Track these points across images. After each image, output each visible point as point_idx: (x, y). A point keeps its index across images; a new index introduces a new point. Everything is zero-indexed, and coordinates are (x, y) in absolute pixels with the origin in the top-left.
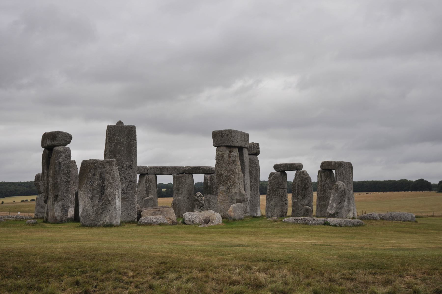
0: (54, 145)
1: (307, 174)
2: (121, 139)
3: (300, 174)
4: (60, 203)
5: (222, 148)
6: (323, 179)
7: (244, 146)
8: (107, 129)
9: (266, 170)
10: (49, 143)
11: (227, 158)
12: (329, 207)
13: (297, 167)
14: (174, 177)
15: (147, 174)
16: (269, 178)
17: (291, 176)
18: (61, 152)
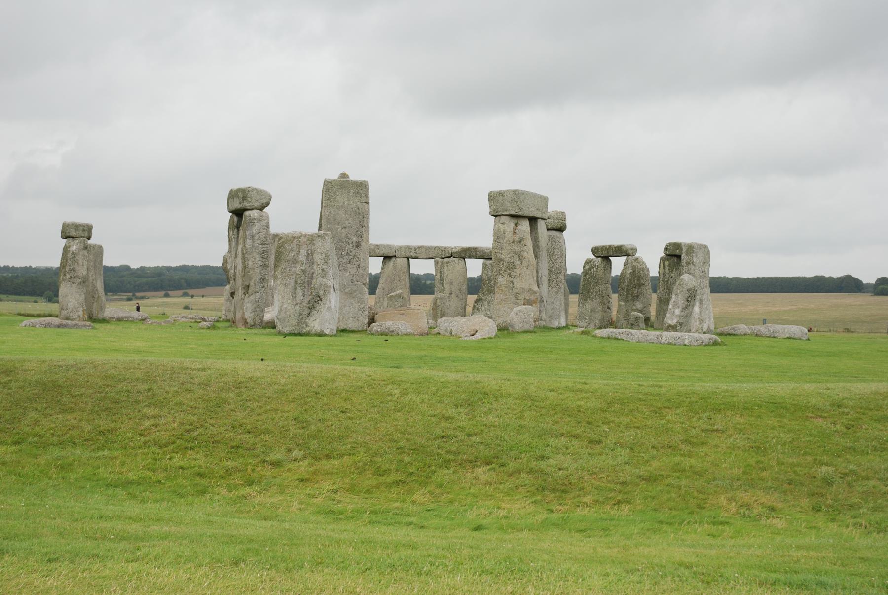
4: (252, 297)
5: (503, 219)
7: (538, 216)
10: (237, 205)
11: (511, 234)
14: (436, 263)
17: (618, 265)
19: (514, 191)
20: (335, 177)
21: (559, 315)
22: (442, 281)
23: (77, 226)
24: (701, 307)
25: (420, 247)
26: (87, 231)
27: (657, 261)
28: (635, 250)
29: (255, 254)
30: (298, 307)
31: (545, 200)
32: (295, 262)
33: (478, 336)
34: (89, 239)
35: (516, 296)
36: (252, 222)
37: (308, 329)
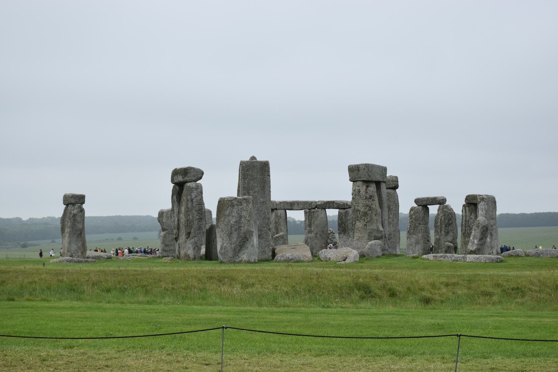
1: (451, 209)
2: (255, 174)
3: (443, 209)
4: (192, 240)
5: (359, 183)
6: (468, 214)
7: (381, 180)
8: (241, 164)
9: (406, 205)
10: (180, 179)
11: (364, 193)
12: (470, 244)
14: (306, 213)
15: (276, 209)
17: (433, 210)
18: (193, 188)
19: (366, 165)
20: (247, 159)
23: (74, 196)
24: (491, 238)
26: (81, 199)
27: (461, 208)
33: (348, 261)
35: (370, 235)
36: (191, 190)
37: (240, 259)
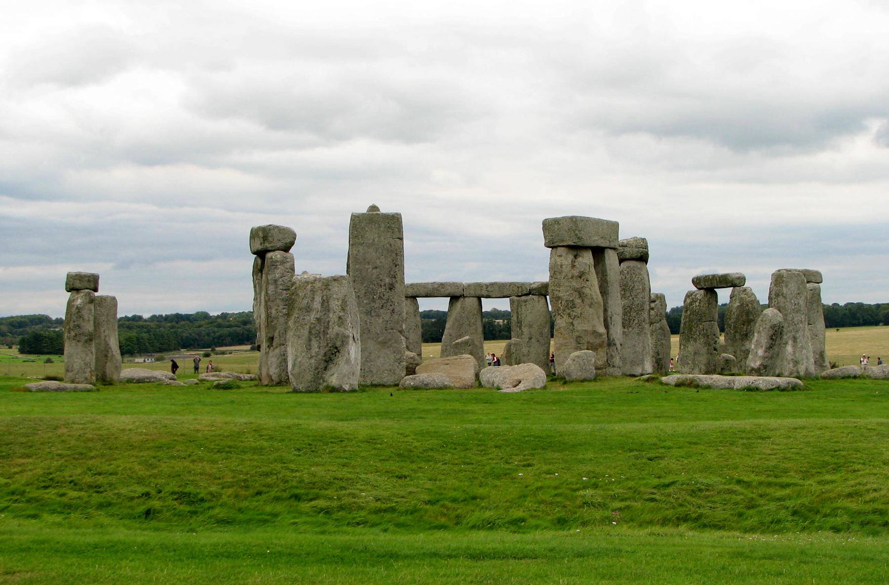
0: (270, 248)
1: (753, 294)
4: (277, 351)
5: (561, 250)
7: (603, 245)
10: (258, 246)
13: (733, 282)
14: (512, 302)
16: (685, 301)
17: (724, 295)
18: (277, 261)
19: (572, 218)
21: (642, 361)
22: (519, 323)
23: (79, 277)
24: (794, 346)
25: (492, 284)
26: (92, 282)
28: (742, 280)
29: (278, 301)
30: (313, 361)
31: (614, 226)
32: (308, 309)
33: (521, 387)
34: (96, 290)
35: (578, 340)
36: (274, 264)
